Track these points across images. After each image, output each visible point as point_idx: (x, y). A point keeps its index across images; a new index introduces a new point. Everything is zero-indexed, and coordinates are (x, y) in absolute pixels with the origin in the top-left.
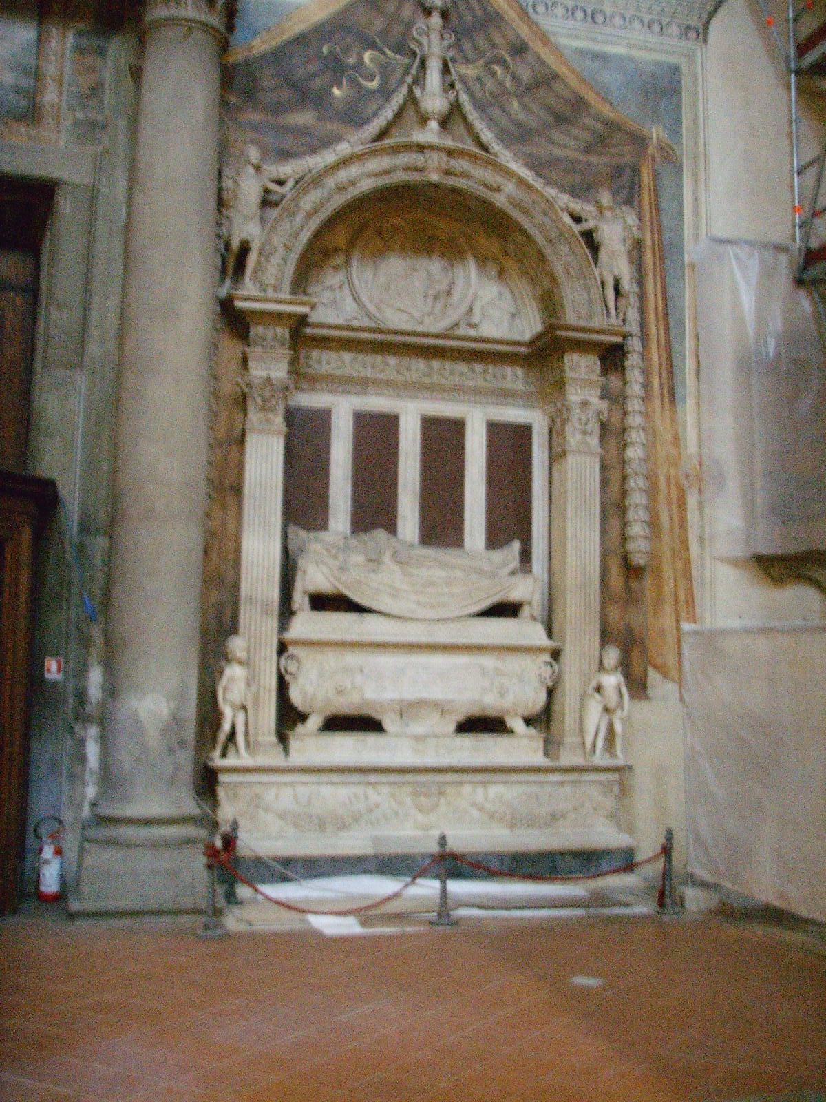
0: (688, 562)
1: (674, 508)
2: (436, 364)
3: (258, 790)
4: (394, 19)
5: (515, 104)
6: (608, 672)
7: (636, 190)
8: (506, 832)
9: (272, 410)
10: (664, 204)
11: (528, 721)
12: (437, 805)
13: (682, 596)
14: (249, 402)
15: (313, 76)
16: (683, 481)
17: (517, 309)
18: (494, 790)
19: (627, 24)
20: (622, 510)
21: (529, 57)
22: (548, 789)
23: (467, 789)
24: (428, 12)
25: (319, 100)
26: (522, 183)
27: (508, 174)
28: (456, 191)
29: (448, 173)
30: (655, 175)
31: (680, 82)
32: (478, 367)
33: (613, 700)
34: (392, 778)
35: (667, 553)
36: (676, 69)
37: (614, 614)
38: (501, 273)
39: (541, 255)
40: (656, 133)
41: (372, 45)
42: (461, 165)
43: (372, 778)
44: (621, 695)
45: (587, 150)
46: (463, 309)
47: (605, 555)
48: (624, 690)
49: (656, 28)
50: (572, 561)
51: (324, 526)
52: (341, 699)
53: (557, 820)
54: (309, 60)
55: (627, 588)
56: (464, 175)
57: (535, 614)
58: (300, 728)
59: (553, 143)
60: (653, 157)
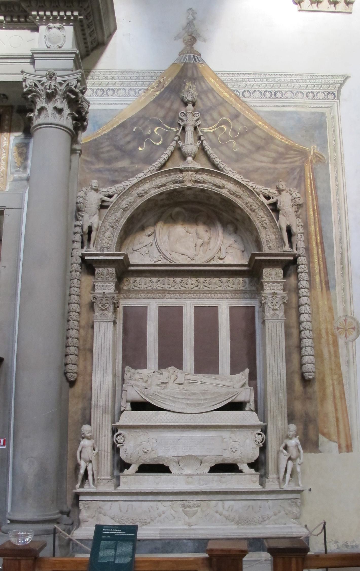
0: (341, 375)
1: (331, 346)
2: (201, 279)
4: (169, 109)
5: (234, 143)
6: (291, 439)
7: (303, 178)
8: (236, 527)
9: (106, 309)
10: (319, 184)
11: (251, 465)
13: (337, 394)
14: (96, 307)
15: (129, 142)
16: (336, 331)
17: (245, 247)
18: (227, 504)
19: (294, 96)
20: (300, 348)
21: (241, 119)
22: (259, 502)
23: (213, 503)
24: (186, 104)
25: (130, 154)
26: (237, 183)
27: (230, 179)
28: (203, 190)
29: (196, 182)
30: (313, 170)
31: (325, 122)
32: (224, 279)
33: (294, 453)
34: (171, 498)
35: (327, 372)
36: (323, 114)
37: (298, 406)
38: (236, 231)
39: (249, 218)
40: (313, 149)
41: (159, 124)
42: (205, 177)
43: (161, 498)
45: (275, 161)
46: (216, 250)
47: (289, 375)
48: (300, 447)
49: (311, 95)
51: (145, 367)
52: (145, 455)
53: (265, 520)
54: (127, 135)
55: (305, 392)
56: (204, 182)
57: (252, 409)
58: (126, 472)
59: (254, 160)
60: (311, 161)
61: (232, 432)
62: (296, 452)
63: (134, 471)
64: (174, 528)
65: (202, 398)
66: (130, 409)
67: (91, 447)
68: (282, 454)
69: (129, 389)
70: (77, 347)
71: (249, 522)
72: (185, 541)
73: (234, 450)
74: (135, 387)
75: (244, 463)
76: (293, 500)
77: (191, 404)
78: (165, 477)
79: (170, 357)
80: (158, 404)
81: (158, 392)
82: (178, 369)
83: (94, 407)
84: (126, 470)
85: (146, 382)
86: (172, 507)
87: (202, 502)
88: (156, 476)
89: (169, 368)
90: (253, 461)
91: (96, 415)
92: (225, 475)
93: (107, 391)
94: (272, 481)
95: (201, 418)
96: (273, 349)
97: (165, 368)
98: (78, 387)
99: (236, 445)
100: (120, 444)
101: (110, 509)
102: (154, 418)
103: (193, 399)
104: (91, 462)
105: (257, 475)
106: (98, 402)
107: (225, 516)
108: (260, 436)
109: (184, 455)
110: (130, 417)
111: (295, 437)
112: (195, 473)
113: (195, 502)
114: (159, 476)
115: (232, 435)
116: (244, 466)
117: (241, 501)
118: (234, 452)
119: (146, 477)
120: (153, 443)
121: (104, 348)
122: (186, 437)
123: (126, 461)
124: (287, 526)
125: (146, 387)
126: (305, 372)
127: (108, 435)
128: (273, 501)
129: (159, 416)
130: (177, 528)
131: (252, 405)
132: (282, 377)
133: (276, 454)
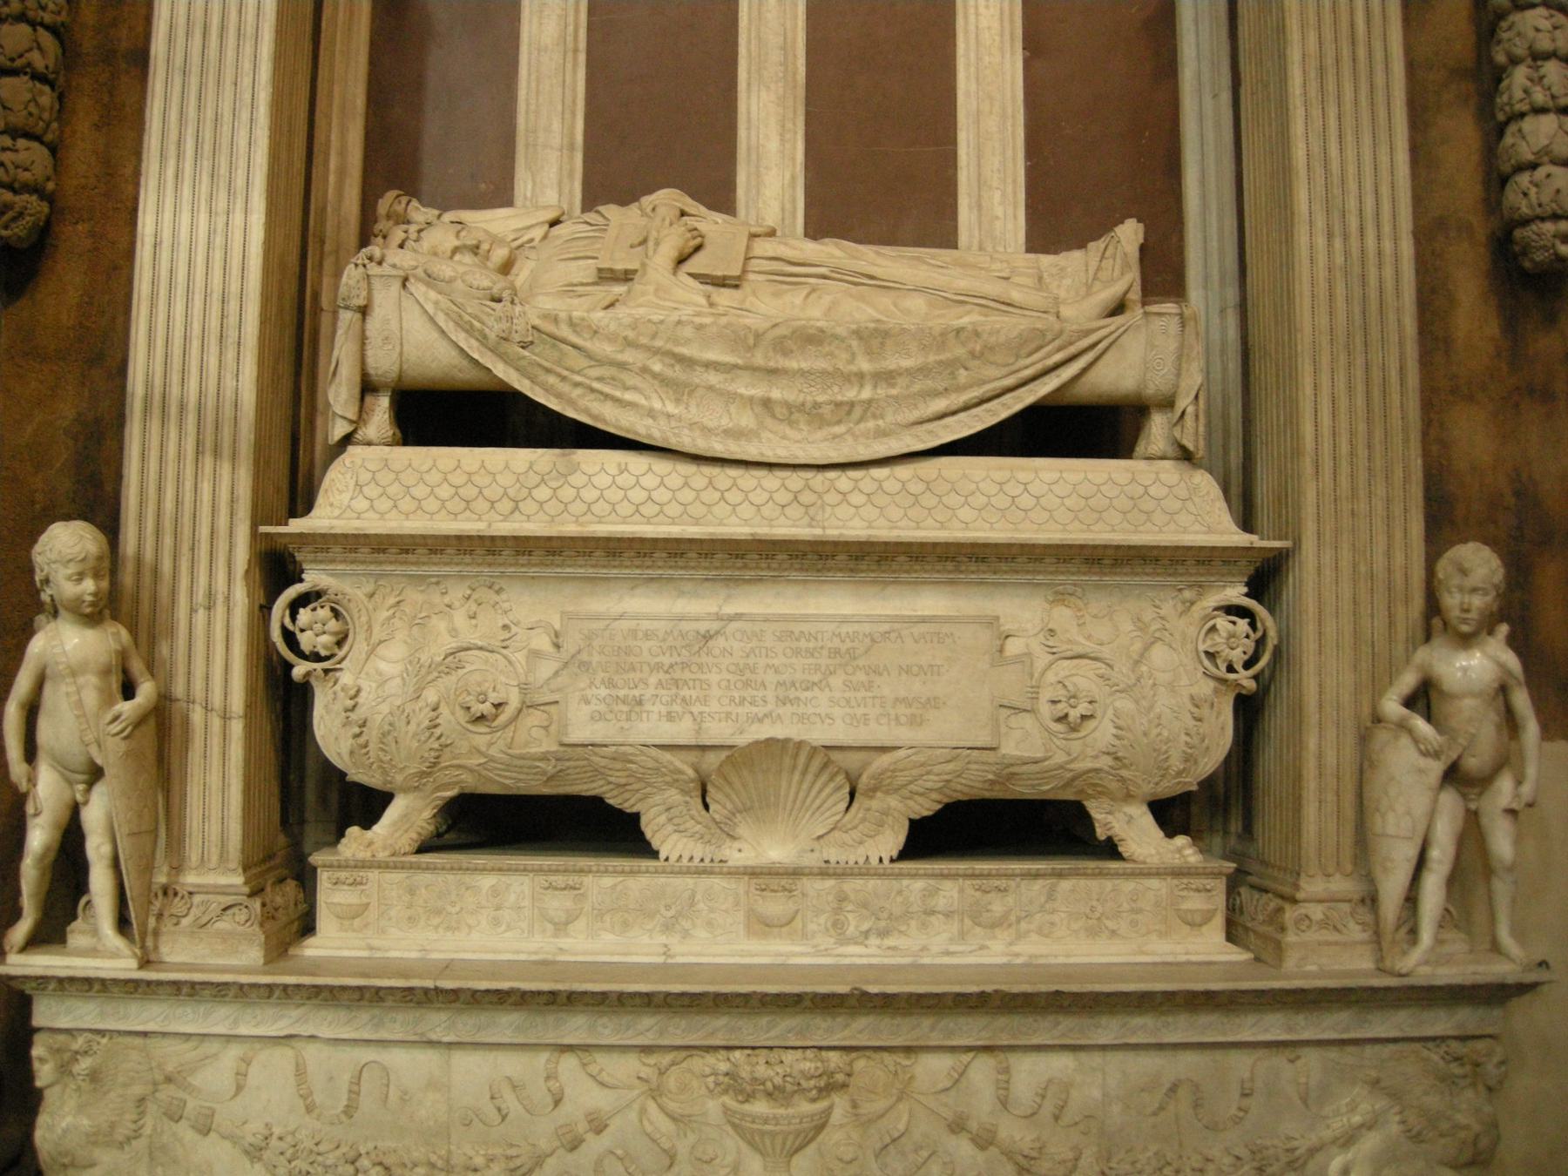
6: (1466, 641)
11: (1171, 814)
12: (821, 1125)
18: (1030, 1072)
22: (1241, 1063)
23: (933, 1068)
34: (647, 1028)
43: (576, 1027)
44: (1510, 722)
47: (1430, 233)
48: (1522, 700)
50: (1312, 246)
51: (501, 195)
57: (1191, 447)
58: (355, 842)
61: (1060, 598)
62: (1498, 727)
63: (407, 840)
65: (865, 365)
66: (399, 434)
67: (105, 672)
68: (1405, 741)
69: (385, 301)
70: (53, 30)
73: (1074, 714)
74: (417, 288)
75: (1129, 797)
76: (1455, 1046)
77: (789, 406)
78: (607, 881)
79: (659, 134)
80: (571, 403)
81: (572, 324)
82: (711, 207)
83: (146, 410)
84: (354, 831)
85: (506, 268)
86: (656, 1093)
87: (861, 1064)
88: (559, 880)
89: (647, 201)
90: (1191, 782)
91: (149, 462)
92: (1012, 876)
93: (233, 306)
94: (1325, 924)
95: (857, 499)
96: (1329, 61)
97: (626, 198)
98: (61, 292)
99: (1084, 678)
100: (316, 657)
101: (239, 1088)
102: (543, 493)
103: (803, 373)
104: (95, 774)
105: (1215, 875)
106: (175, 378)
107: (1008, 1154)
108: (1243, 624)
109: (742, 740)
110: (377, 485)
111: (1491, 632)
112: (811, 860)
113: (807, 1064)
114: (572, 879)
115: (1062, 616)
116: (1130, 819)
118: (1074, 729)
119: (487, 882)
120: (535, 654)
121: (223, 28)
122: (751, 618)
123: (356, 775)
125: (495, 290)
126: (1526, 222)
127: (228, 599)
128: (1333, 1054)
129: (577, 479)
131: (1189, 420)
132: (1387, 245)
133: (1350, 740)
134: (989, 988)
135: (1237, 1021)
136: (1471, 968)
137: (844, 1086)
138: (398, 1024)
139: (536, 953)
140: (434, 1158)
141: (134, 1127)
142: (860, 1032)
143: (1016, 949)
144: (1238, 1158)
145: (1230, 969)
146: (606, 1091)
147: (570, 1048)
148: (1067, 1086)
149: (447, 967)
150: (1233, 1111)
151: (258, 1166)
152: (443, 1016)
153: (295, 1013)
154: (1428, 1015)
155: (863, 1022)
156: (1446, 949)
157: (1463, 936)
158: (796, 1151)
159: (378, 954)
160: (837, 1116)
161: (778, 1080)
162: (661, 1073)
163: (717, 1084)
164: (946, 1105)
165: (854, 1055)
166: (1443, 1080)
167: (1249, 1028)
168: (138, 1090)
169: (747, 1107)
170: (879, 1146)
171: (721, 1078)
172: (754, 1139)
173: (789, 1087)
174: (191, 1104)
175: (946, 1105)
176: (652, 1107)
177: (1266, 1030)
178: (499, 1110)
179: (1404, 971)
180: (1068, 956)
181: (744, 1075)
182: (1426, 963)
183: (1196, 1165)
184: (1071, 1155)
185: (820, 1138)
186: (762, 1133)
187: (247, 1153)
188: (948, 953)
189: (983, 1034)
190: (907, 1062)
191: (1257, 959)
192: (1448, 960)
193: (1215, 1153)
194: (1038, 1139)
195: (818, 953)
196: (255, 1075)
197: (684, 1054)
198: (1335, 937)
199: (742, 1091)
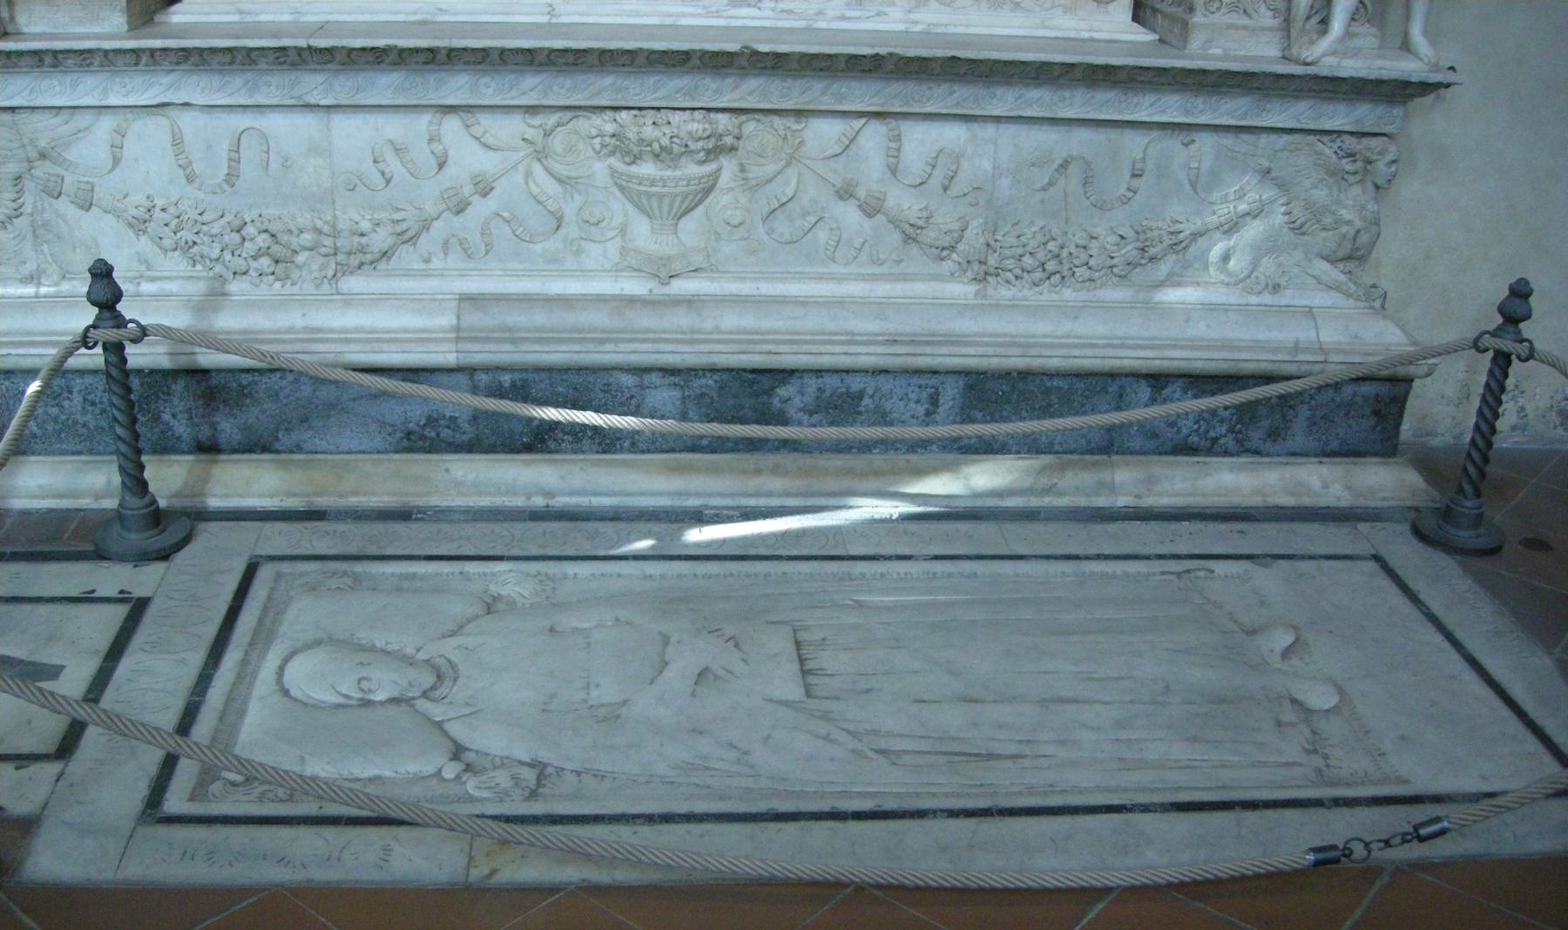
3: (44, 129)
8: (961, 290)
18: (921, 141)
22: (1134, 143)
23: (824, 133)
34: (530, 87)
43: (457, 87)
53: (1152, 259)
64: (556, 287)
71: (1051, 266)
72: (628, 380)
76: (1350, 142)
86: (541, 155)
87: (750, 127)
101: (116, 161)
113: (694, 125)
117: (1011, 130)
124: (1286, 298)
128: (1228, 140)
130: (573, 287)
134: (883, 51)
135: (1135, 100)
136: (1379, 63)
137: (733, 149)
138: (273, 88)
139: (414, 13)
140: (319, 224)
141: (14, 205)
142: (750, 94)
143: (915, 16)
144: (1122, 237)
145: (1135, 48)
146: (491, 153)
147: (452, 109)
148: (958, 158)
149: (322, 28)
150: (1123, 190)
151: (143, 239)
152: (319, 78)
153: (166, 80)
154: (1330, 108)
155: (753, 83)
156: (1358, 42)
157: (1374, 30)
158: (685, 213)
159: (249, 19)
160: (725, 179)
161: (665, 141)
162: (547, 134)
163: (603, 146)
164: (835, 171)
165: (744, 118)
166: (1332, 174)
167: (1145, 107)
168: (13, 168)
169: (634, 169)
170: (766, 210)
171: (608, 140)
172: (641, 199)
173: (676, 148)
174: (69, 179)
175: (835, 171)
176: (537, 168)
177: (1163, 112)
178: (383, 174)
179: (1309, 60)
180: (968, 26)
181: (630, 135)
182: (1334, 53)
183: (1081, 242)
184: (957, 226)
185: (707, 202)
186: (649, 195)
187: (131, 225)
188: (844, 18)
189: (875, 100)
190: (796, 127)
191: (1161, 41)
192: (1356, 53)
193: (1099, 231)
194: (926, 208)
195: (709, 15)
196: (131, 148)
197: (569, 114)
198: (1245, 21)
199: (628, 153)
